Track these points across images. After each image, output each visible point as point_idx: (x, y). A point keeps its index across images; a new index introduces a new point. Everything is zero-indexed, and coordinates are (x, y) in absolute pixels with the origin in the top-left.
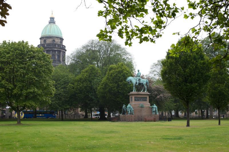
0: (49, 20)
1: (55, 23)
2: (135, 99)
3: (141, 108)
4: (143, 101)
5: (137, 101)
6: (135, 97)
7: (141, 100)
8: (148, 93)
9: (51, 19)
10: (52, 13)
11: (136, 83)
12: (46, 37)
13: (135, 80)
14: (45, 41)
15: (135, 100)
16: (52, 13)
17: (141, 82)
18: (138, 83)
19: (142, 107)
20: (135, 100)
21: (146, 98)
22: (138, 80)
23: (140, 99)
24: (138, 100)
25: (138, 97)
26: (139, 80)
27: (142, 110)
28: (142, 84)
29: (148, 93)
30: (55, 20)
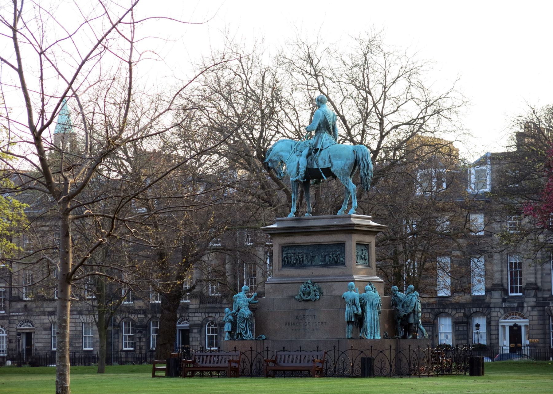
2: (283, 260)
3: (301, 305)
4: (326, 265)
6: (284, 247)
7: (318, 260)
8: (372, 223)
15: (286, 264)
19: (306, 299)
20: (286, 264)
21: (341, 246)
22: (305, 152)
24: (300, 264)
25: (300, 246)
27: (304, 317)
29: (372, 223)
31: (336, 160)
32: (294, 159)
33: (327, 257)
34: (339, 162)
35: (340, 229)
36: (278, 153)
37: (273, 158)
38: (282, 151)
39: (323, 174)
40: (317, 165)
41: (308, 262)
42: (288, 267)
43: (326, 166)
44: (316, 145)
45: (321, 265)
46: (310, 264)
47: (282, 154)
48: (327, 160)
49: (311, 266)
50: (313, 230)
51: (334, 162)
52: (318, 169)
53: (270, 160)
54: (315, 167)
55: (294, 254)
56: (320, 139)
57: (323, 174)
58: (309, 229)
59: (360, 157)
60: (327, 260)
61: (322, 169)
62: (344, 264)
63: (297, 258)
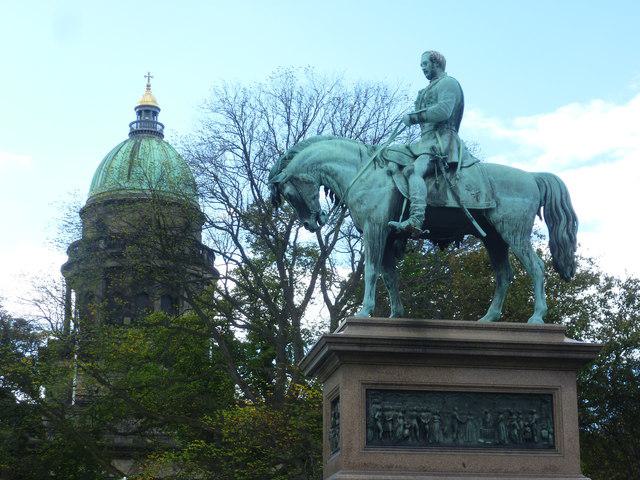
0: (134, 117)
1: (160, 135)
2: (371, 426)
4: (499, 445)
5: (400, 442)
6: (373, 393)
9: (139, 113)
10: (148, 86)
11: (399, 204)
12: (107, 203)
13: (380, 174)
14: (100, 225)
15: (380, 435)
16: (148, 86)
17: (468, 200)
18: (419, 206)
20: (380, 435)
21: (544, 400)
22: (421, 165)
23: (457, 426)
24: (422, 437)
26: (428, 175)
28: (482, 215)
30: (161, 118)
31: (509, 195)
32: (381, 181)
33: (502, 425)
34: (520, 200)
35: (556, 355)
36: (320, 163)
37: (303, 175)
38: (335, 160)
39: (475, 223)
40: (457, 199)
41: (445, 435)
42: (382, 445)
43: (482, 204)
44: (449, 151)
45: (484, 447)
46: (449, 440)
47: (336, 167)
48: (484, 190)
49: (455, 446)
50: (479, 353)
51: (505, 200)
52: (459, 211)
53: (293, 180)
54: (451, 203)
55: (404, 412)
56: (455, 142)
57: (475, 223)
58: (470, 348)
59: (559, 198)
60: (504, 434)
61: (470, 210)
62: (551, 447)
63: (415, 422)
